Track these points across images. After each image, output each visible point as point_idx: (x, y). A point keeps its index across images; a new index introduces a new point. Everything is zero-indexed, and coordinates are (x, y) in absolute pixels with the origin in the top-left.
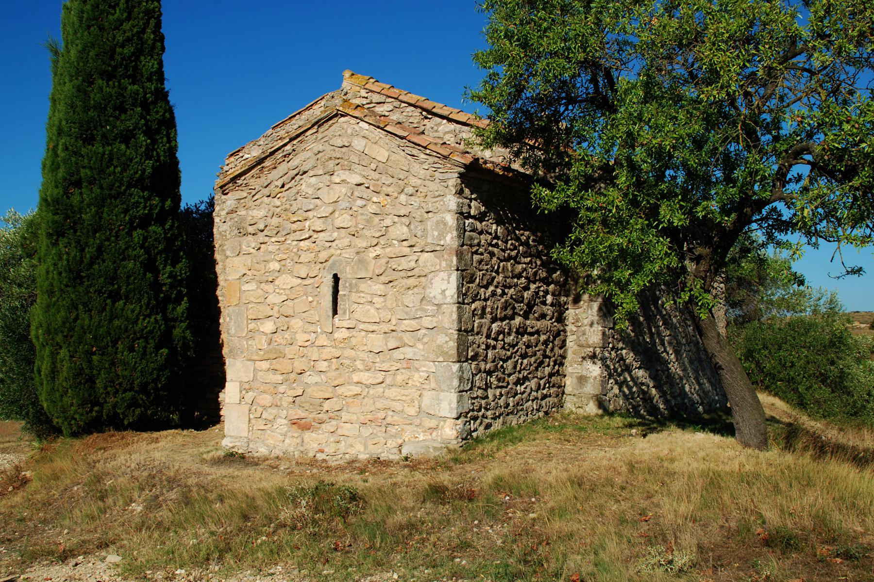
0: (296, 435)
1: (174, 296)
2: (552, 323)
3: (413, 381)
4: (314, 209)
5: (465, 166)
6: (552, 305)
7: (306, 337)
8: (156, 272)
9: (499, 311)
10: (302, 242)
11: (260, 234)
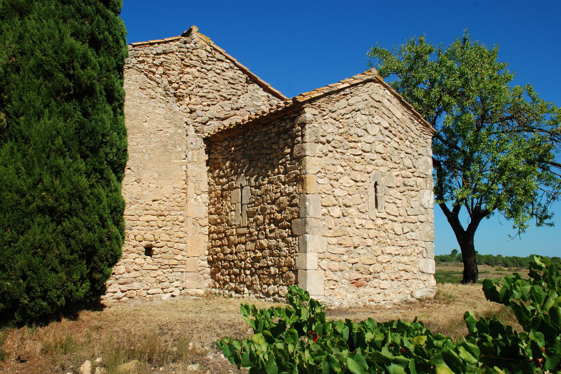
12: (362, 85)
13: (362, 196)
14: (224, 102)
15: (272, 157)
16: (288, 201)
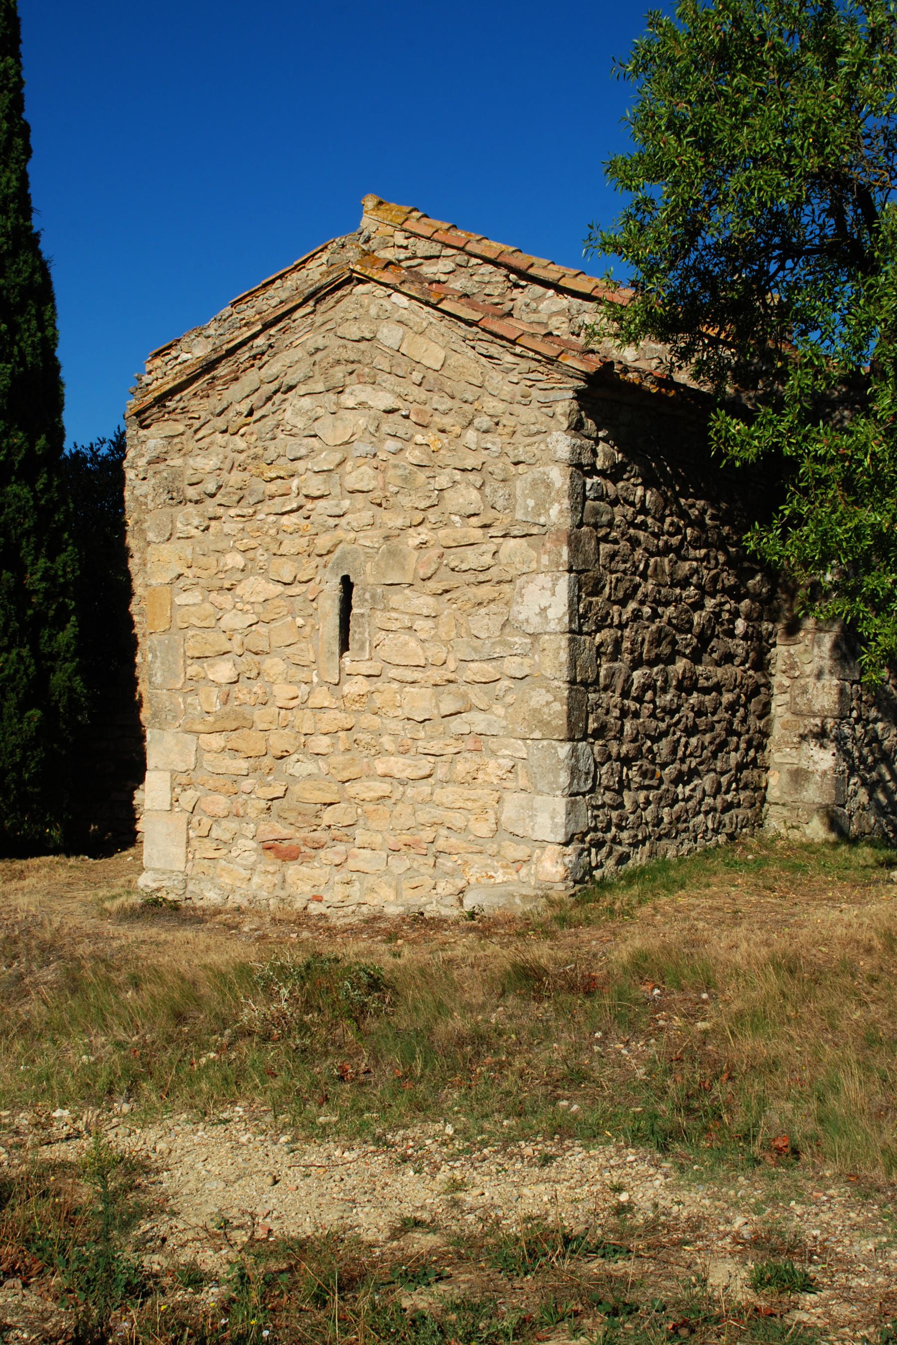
0: (271, 869)
1: (52, 613)
2: (745, 672)
3: (486, 774)
4: (307, 456)
5: (588, 377)
6: (745, 637)
7: (292, 690)
8: (20, 570)
9: (646, 647)
10: (286, 517)
11: (209, 501)
12: (307, 309)
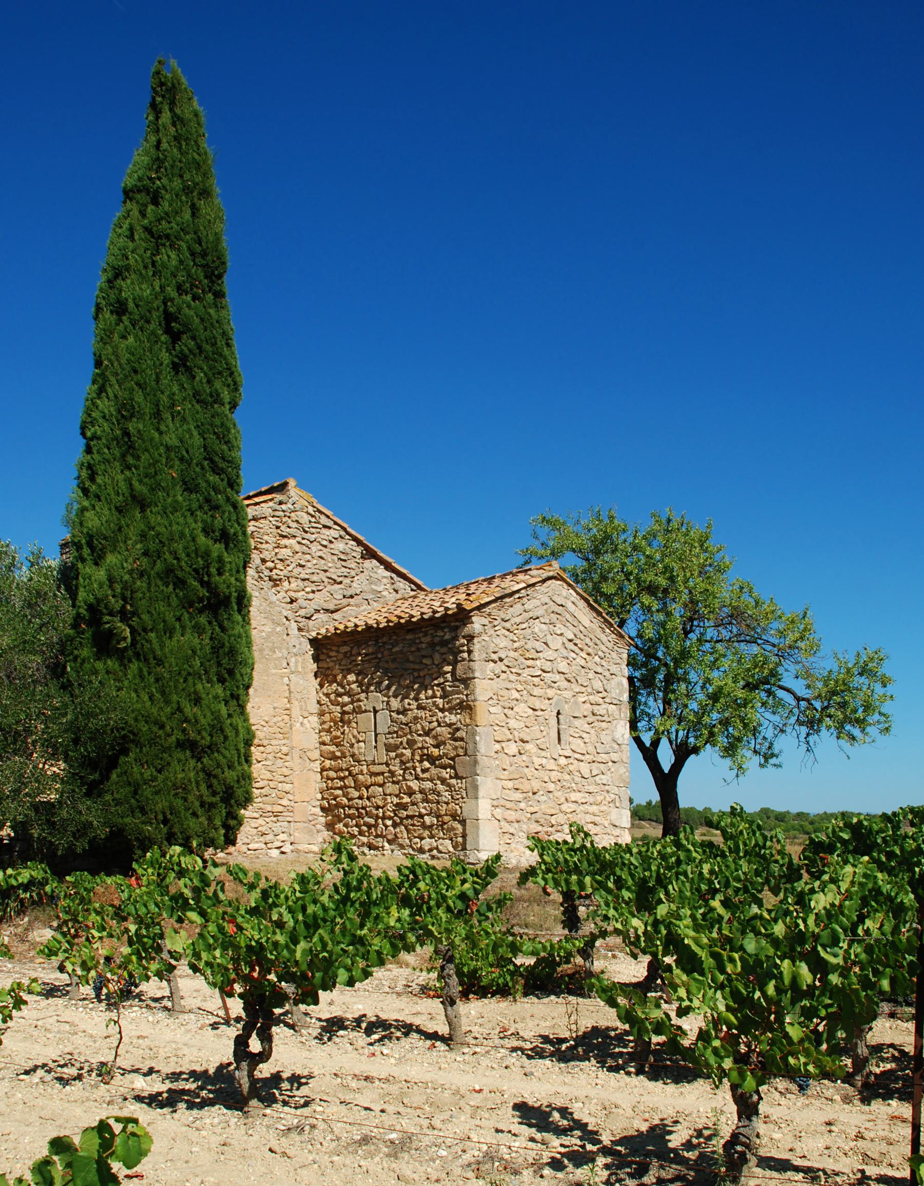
13: (542, 728)
14: (333, 587)
15: (422, 674)
16: (450, 733)
